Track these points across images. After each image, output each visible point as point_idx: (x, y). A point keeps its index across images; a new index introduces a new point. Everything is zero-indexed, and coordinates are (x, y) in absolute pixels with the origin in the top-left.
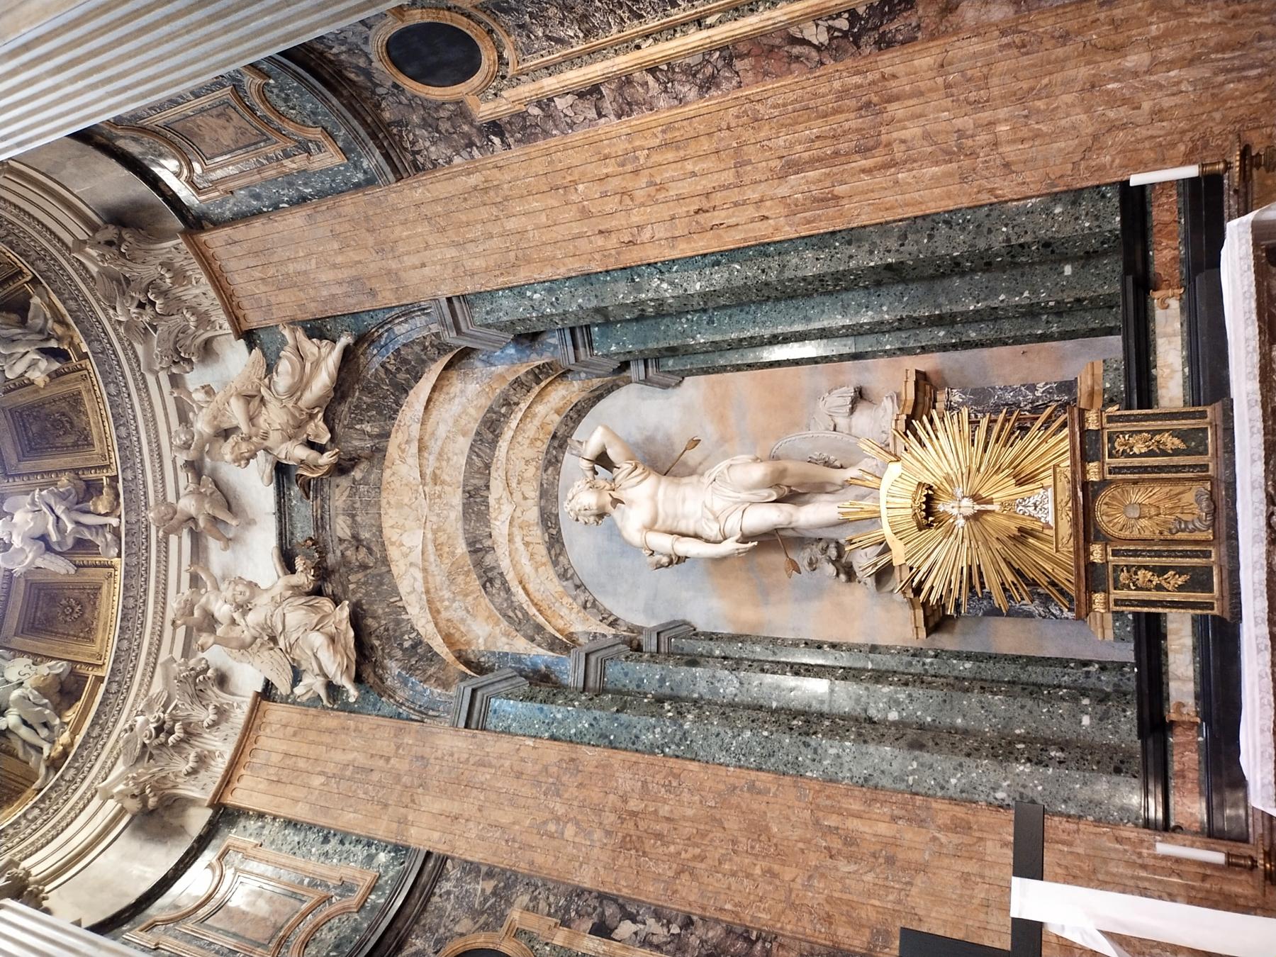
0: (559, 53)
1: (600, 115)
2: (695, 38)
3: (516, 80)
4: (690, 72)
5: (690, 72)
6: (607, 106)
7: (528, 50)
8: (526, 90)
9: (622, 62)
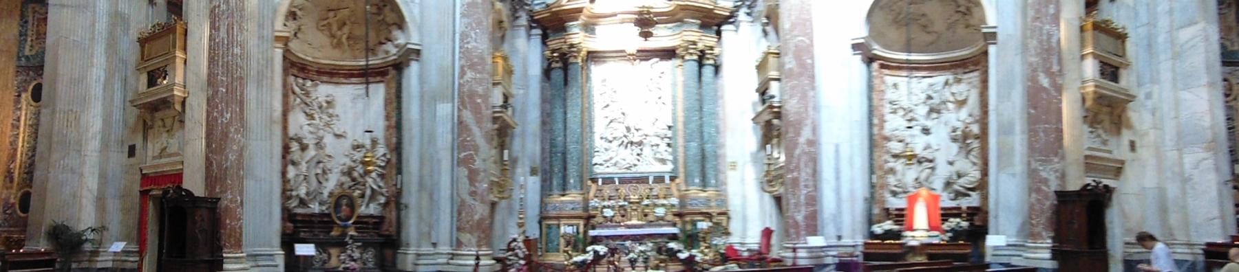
0: (28, 117)
1: (14, 120)
2: (20, 145)
3: (27, 106)
4: (15, 141)
5: (15, 141)
6: (14, 122)
7: (31, 113)
8: (24, 107)
9: (22, 129)
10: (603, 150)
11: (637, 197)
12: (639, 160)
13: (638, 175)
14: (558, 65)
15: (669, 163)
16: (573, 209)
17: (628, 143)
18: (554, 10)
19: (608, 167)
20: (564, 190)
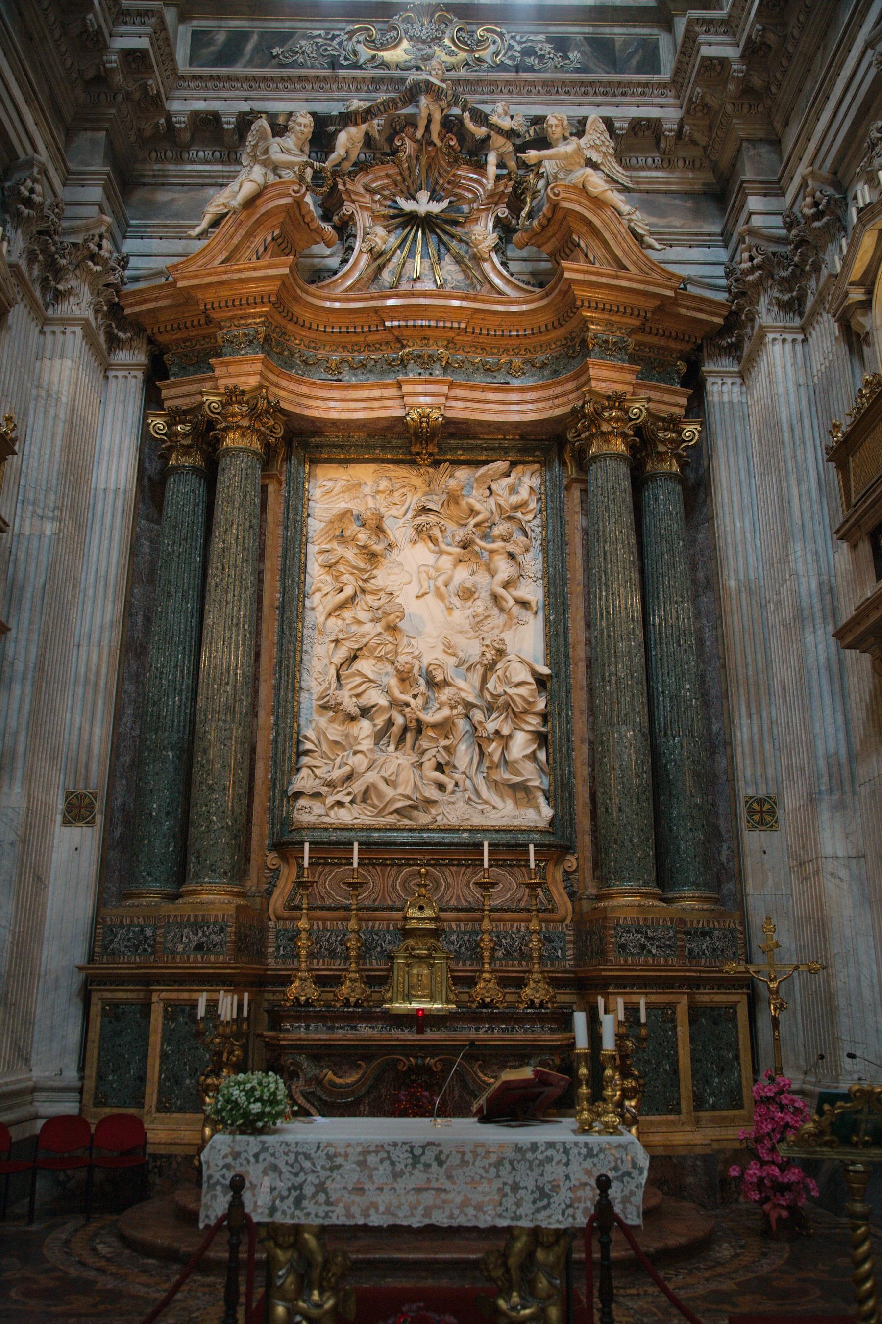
10: (325, 747)
11: (429, 913)
12: (441, 787)
13: (436, 837)
14: (187, 461)
15: (542, 800)
16: (199, 947)
17: (405, 729)
18: (180, 284)
19: (340, 804)
20: (181, 875)
